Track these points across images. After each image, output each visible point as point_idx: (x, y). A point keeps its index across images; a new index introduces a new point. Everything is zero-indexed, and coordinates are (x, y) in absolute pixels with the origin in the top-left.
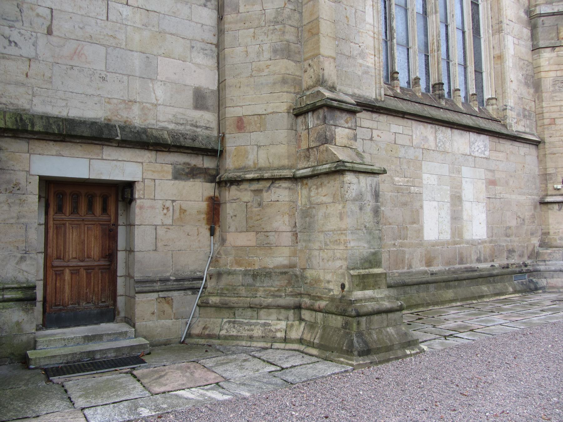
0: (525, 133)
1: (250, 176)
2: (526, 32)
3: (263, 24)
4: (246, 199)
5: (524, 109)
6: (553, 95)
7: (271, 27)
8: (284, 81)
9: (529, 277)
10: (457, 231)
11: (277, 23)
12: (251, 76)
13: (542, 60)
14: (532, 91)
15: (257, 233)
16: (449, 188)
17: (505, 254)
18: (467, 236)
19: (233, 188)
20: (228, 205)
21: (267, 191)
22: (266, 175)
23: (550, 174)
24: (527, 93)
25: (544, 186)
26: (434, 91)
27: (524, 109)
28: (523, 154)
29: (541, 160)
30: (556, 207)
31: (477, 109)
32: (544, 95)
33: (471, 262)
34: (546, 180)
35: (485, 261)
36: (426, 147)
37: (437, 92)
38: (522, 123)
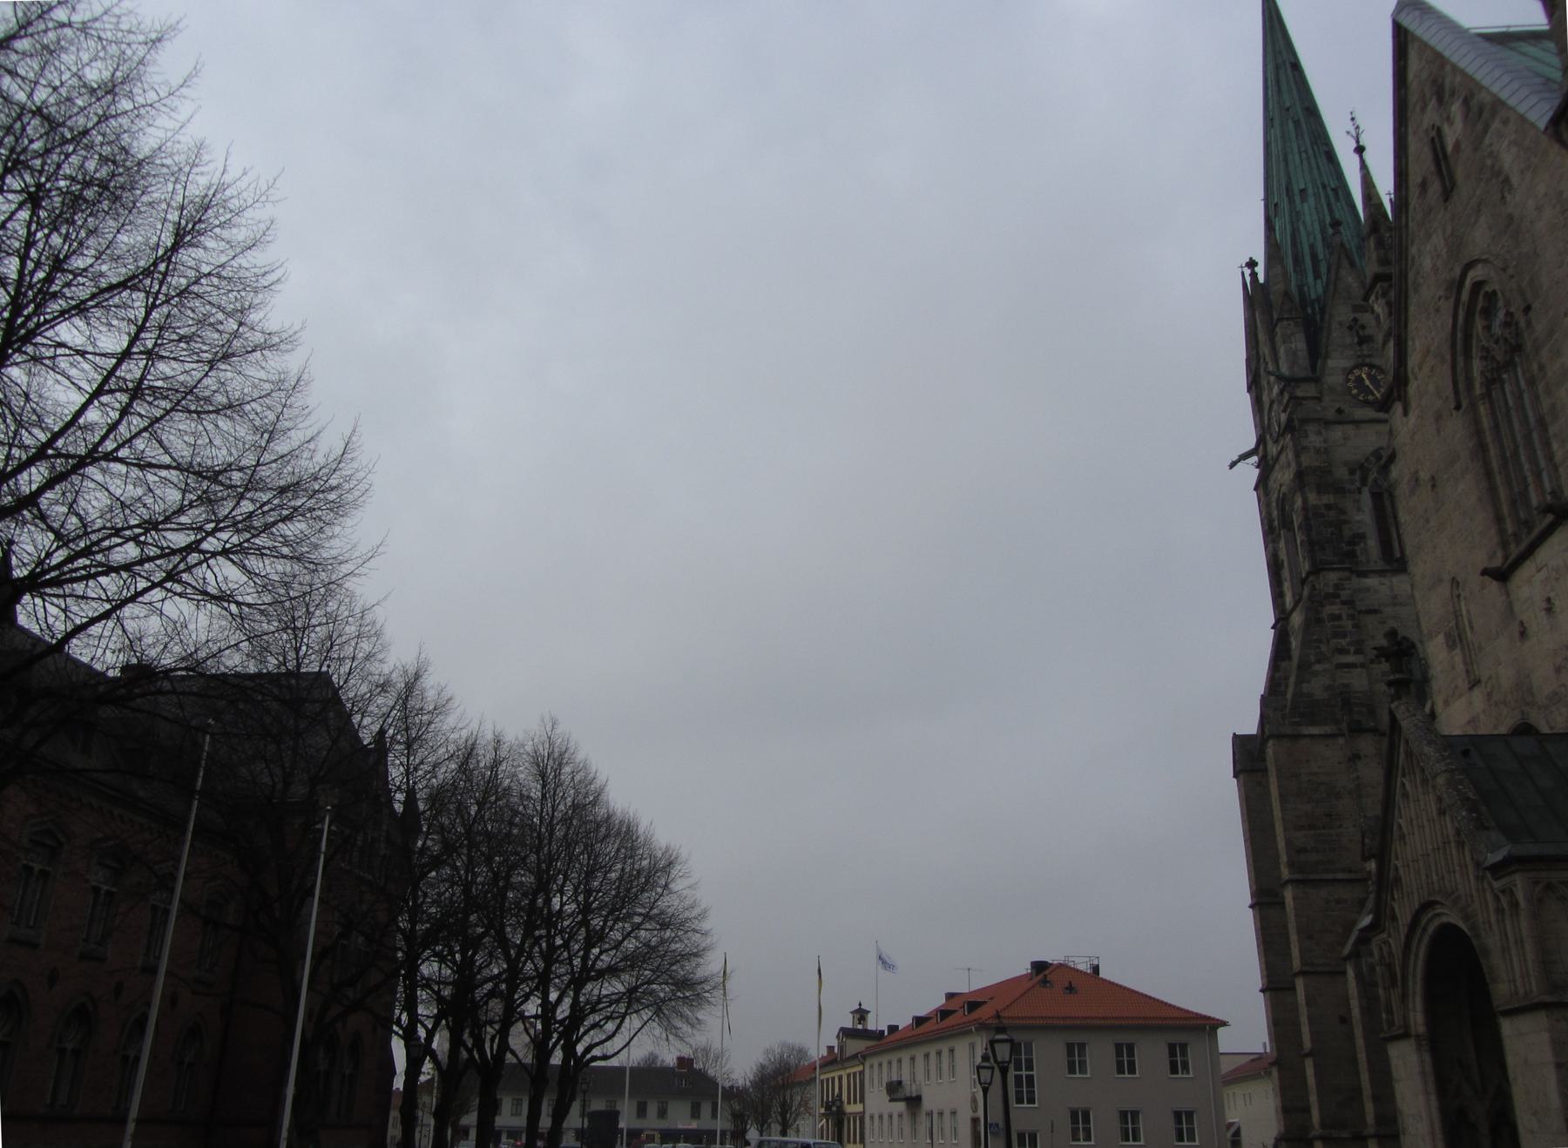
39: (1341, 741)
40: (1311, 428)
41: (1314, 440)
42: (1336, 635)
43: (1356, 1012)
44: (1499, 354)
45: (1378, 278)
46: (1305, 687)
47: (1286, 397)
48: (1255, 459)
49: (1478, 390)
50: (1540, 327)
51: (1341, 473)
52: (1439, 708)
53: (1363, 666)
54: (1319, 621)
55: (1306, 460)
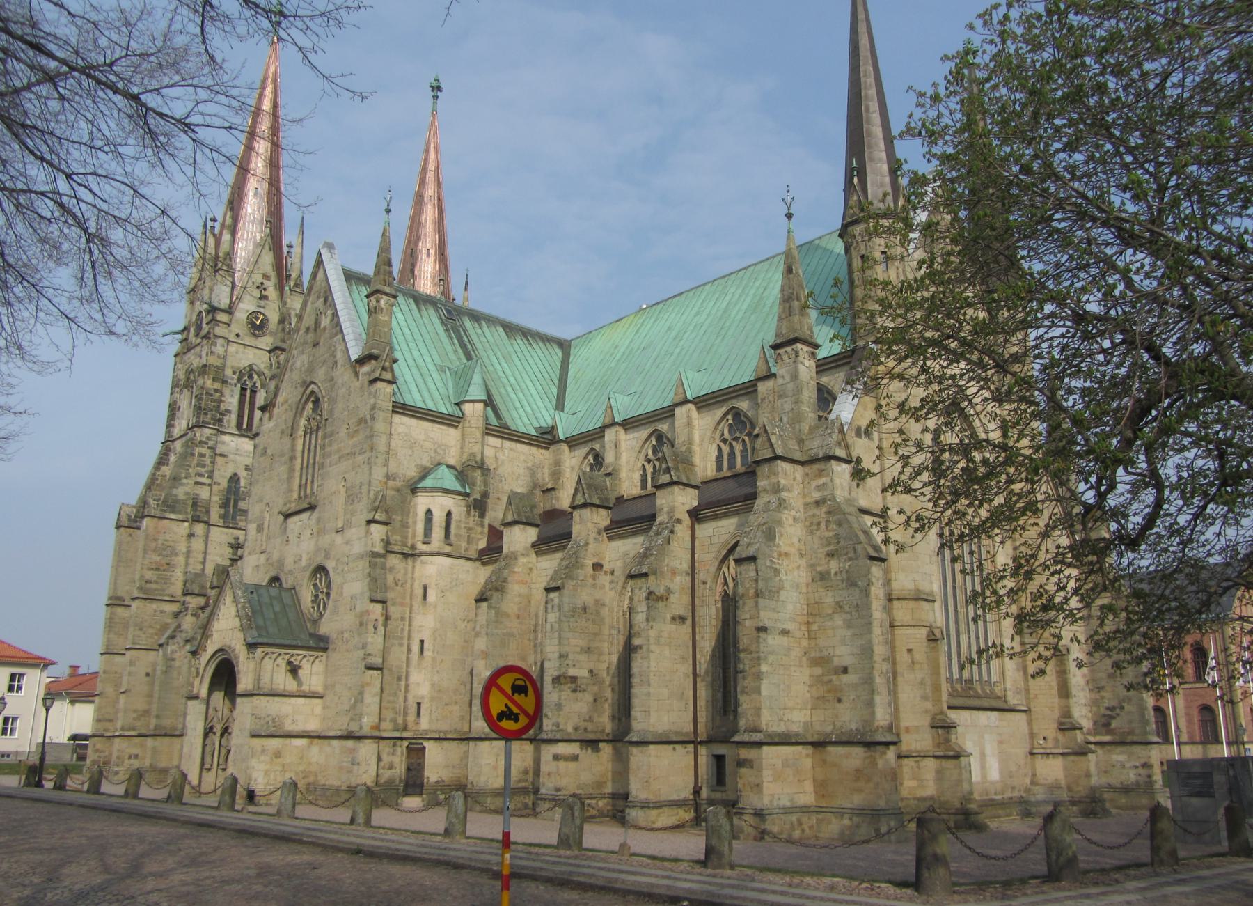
10: (984, 776)
29: (1030, 722)
39: (186, 524)
40: (220, 341)
41: (219, 349)
42: (198, 465)
43: (158, 673)
44: (314, 424)
45: (277, 348)
46: (175, 491)
47: (210, 317)
48: (179, 336)
49: (301, 432)
50: (329, 430)
51: (228, 372)
52: (246, 554)
53: (210, 485)
54: (193, 455)
55: (214, 361)
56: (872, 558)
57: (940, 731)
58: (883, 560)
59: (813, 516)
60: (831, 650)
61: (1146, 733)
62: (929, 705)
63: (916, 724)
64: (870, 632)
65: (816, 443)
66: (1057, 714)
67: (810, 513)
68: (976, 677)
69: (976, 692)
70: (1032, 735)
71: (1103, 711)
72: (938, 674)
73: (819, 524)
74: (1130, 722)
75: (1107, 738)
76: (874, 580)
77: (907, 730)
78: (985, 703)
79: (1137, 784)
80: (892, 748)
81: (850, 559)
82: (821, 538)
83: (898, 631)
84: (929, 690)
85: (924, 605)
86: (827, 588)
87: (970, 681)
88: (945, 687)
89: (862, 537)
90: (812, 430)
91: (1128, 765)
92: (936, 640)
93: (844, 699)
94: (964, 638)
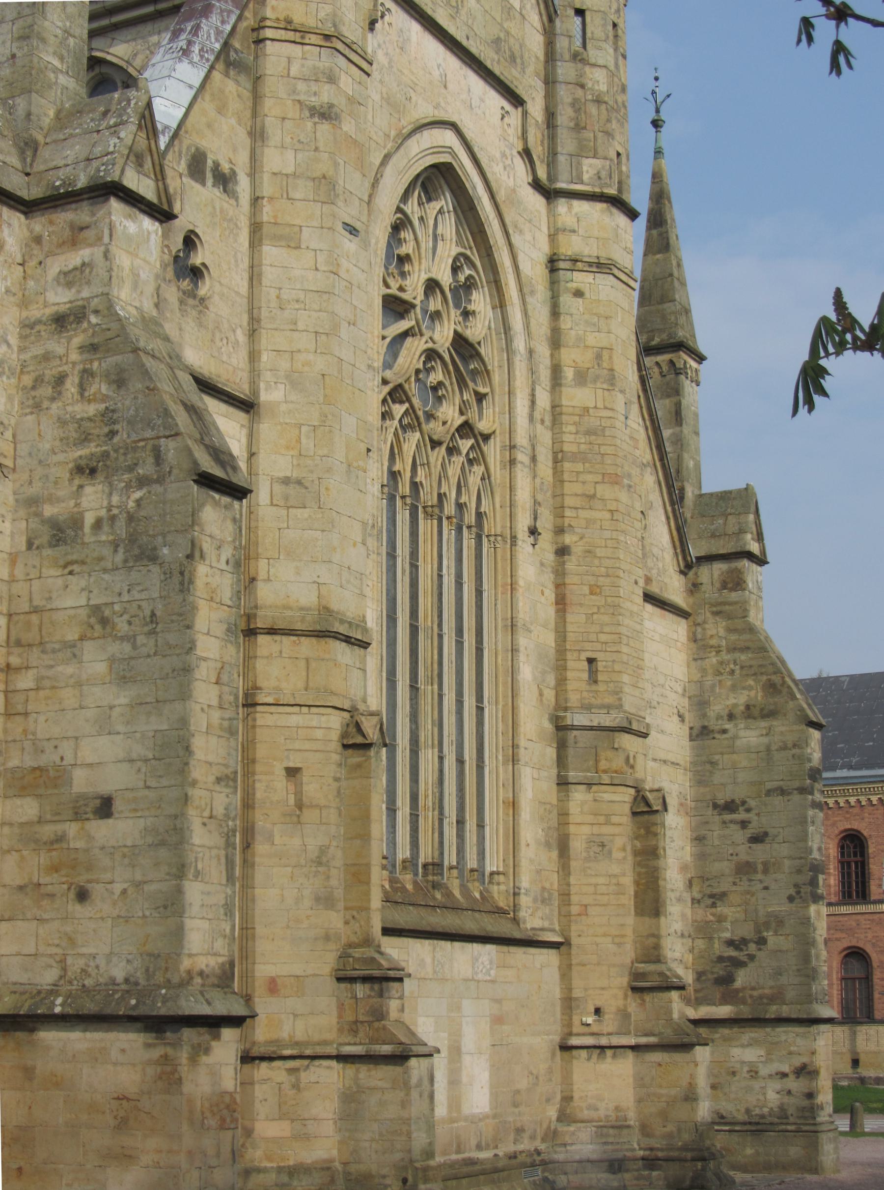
0: (542, 929)
1: (287, 1052)
2: (551, 752)
3: (303, 862)
4: (279, 1080)
5: (544, 889)
6: (587, 865)
7: (314, 869)
8: (327, 938)
9: (543, 1171)
10: (455, 1103)
11: (320, 864)
12: (288, 927)
13: (571, 804)
14: (555, 854)
15: (293, 1121)
16: (446, 1035)
17: (512, 1137)
18: (466, 1110)
19: (264, 1065)
20: (257, 1087)
21: (305, 1070)
22: (308, 1052)
23: (576, 999)
24: (550, 858)
25: (566, 1017)
26: (425, 874)
27: (544, 889)
28: (539, 966)
30: (584, 1053)
31: (477, 895)
32: (573, 864)
33: (470, 1150)
34: (570, 1008)
35: (487, 1147)
36: (422, 975)
37: (430, 878)
38: (539, 913)
56: (206, 481)
57: (361, 990)
58: (239, 492)
59: (47, 357)
60: (66, 749)
61: (809, 998)
62: (335, 920)
63: (297, 969)
64: (185, 695)
65: (74, 151)
66: (628, 953)
67: (38, 350)
68: (450, 858)
69: (449, 894)
70: (569, 1003)
71: (718, 948)
72: (365, 837)
73: (60, 380)
74: (778, 973)
75: (724, 1011)
76: (207, 546)
77: (273, 986)
78: (469, 924)
79: (783, 1113)
80: (228, 1034)
81: (143, 482)
82: (62, 422)
83: (264, 718)
84: (337, 879)
85: (342, 652)
86: (68, 567)
87: (436, 866)
88: (378, 877)
89: (182, 419)
90: (62, 119)
91: (764, 1071)
92: (367, 746)
93: (97, 890)
94: (428, 758)
